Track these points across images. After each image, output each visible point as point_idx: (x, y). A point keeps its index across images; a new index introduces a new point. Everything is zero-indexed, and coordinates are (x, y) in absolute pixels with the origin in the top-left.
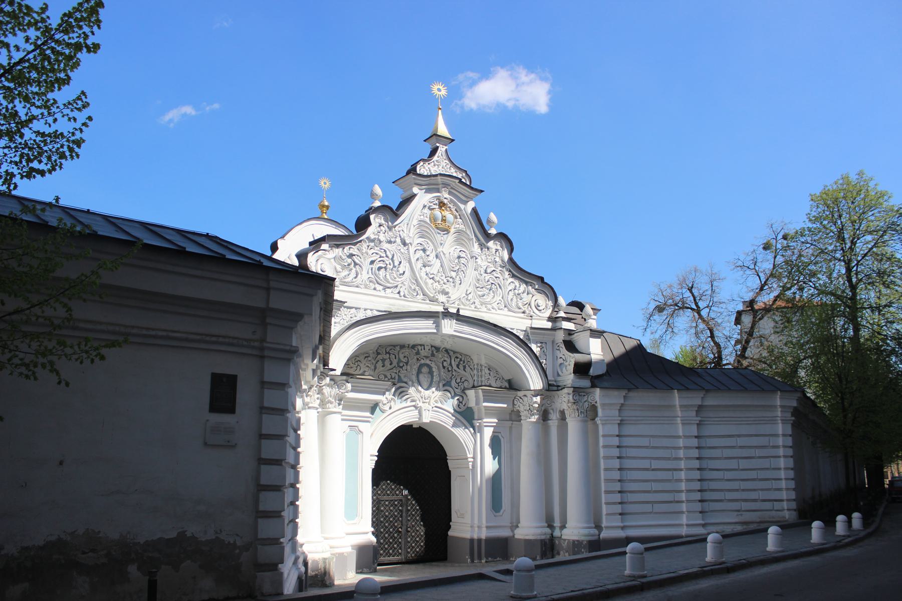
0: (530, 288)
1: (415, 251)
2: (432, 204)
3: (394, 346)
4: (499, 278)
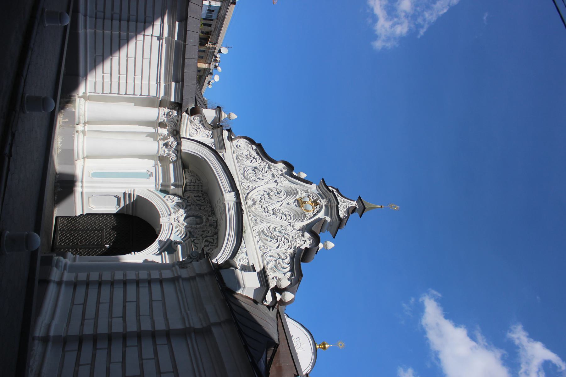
0: (289, 274)
1: (275, 188)
2: (311, 196)
3: (210, 203)
4: (284, 245)
